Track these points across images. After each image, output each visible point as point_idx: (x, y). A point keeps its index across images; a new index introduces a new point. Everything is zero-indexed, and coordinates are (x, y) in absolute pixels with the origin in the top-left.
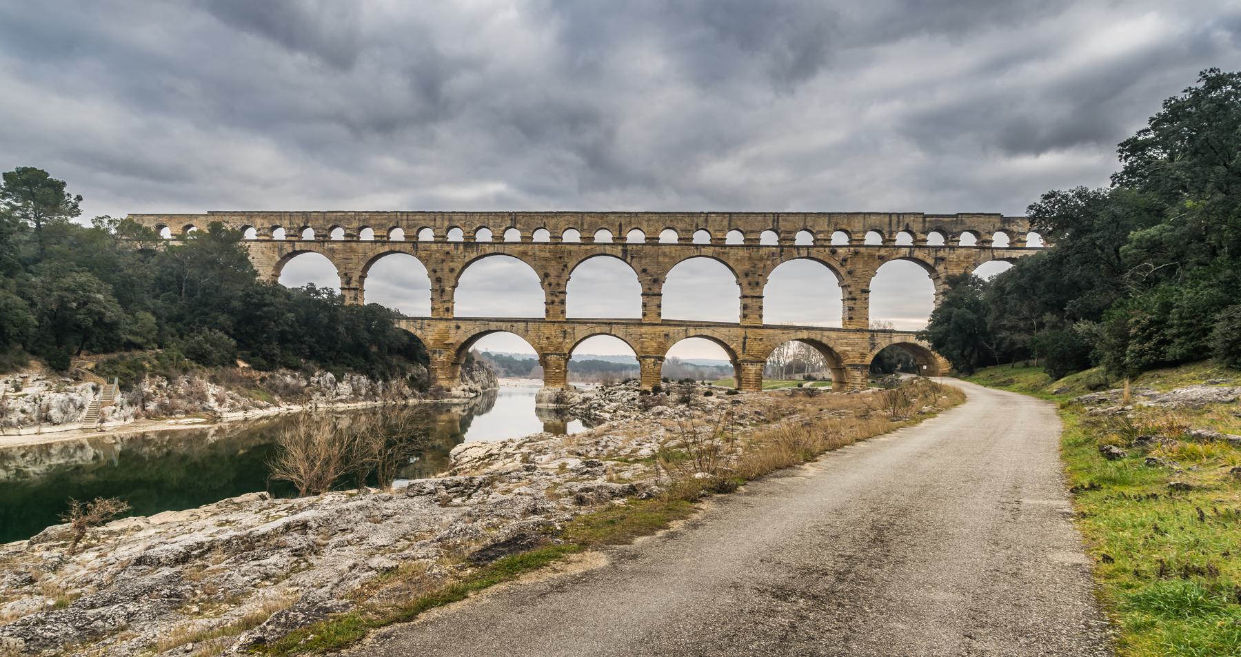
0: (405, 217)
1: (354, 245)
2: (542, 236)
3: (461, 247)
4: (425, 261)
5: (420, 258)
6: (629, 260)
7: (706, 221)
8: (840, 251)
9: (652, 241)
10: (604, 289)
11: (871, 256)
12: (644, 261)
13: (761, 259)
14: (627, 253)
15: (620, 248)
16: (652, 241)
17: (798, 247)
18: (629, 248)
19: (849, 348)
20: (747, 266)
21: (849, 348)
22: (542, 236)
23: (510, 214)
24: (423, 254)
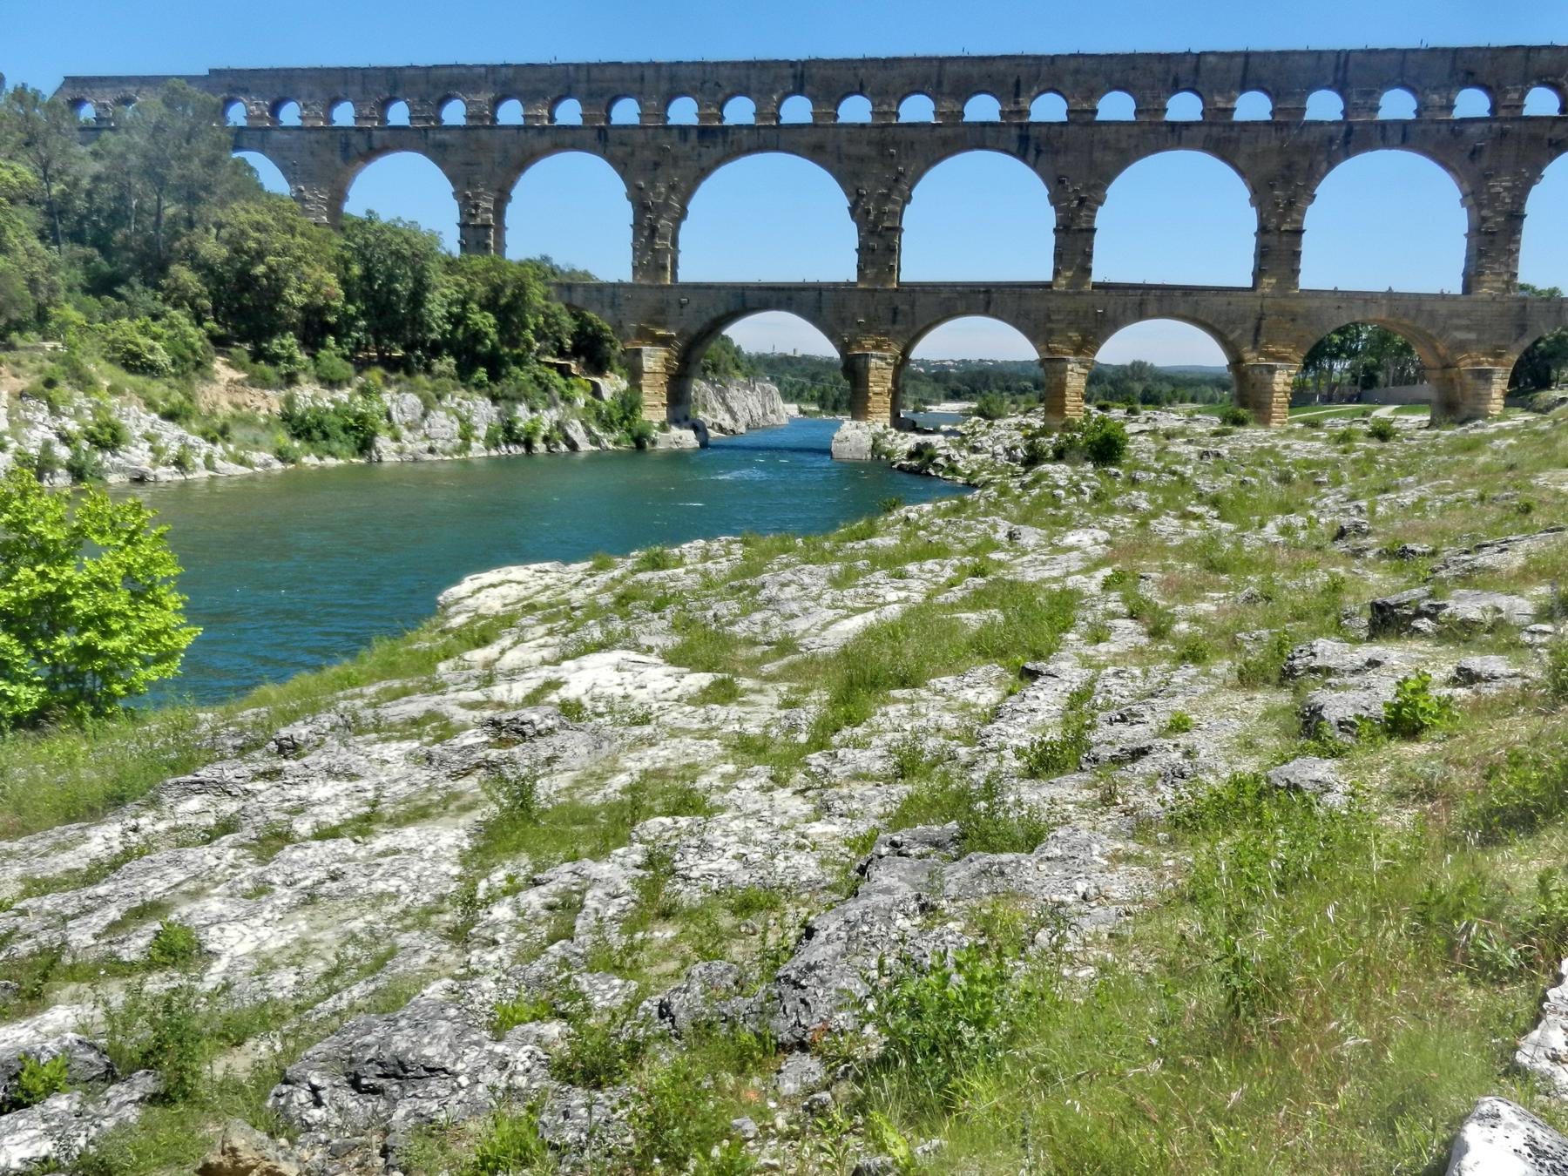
0: (583, 74)
1: (484, 134)
2: (855, 110)
3: (693, 136)
4: (622, 166)
5: (612, 160)
6: (1032, 152)
7: (1197, 70)
8: (1472, 130)
9: (1082, 117)
10: (978, 220)
11: (1535, 139)
12: (1061, 160)
13: (1306, 149)
14: (1025, 141)
15: (1014, 132)
16: (1082, 117)
17: (1384, 125)
18: (1033, 132)
19: (1473, 336)
20: (1273, 165)
21: (1473, 336)
22: (855, 110)
23: (792, 64)
24: (620, 152)
